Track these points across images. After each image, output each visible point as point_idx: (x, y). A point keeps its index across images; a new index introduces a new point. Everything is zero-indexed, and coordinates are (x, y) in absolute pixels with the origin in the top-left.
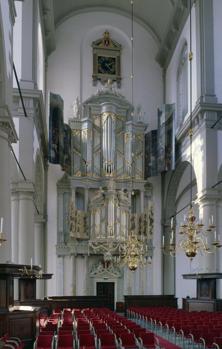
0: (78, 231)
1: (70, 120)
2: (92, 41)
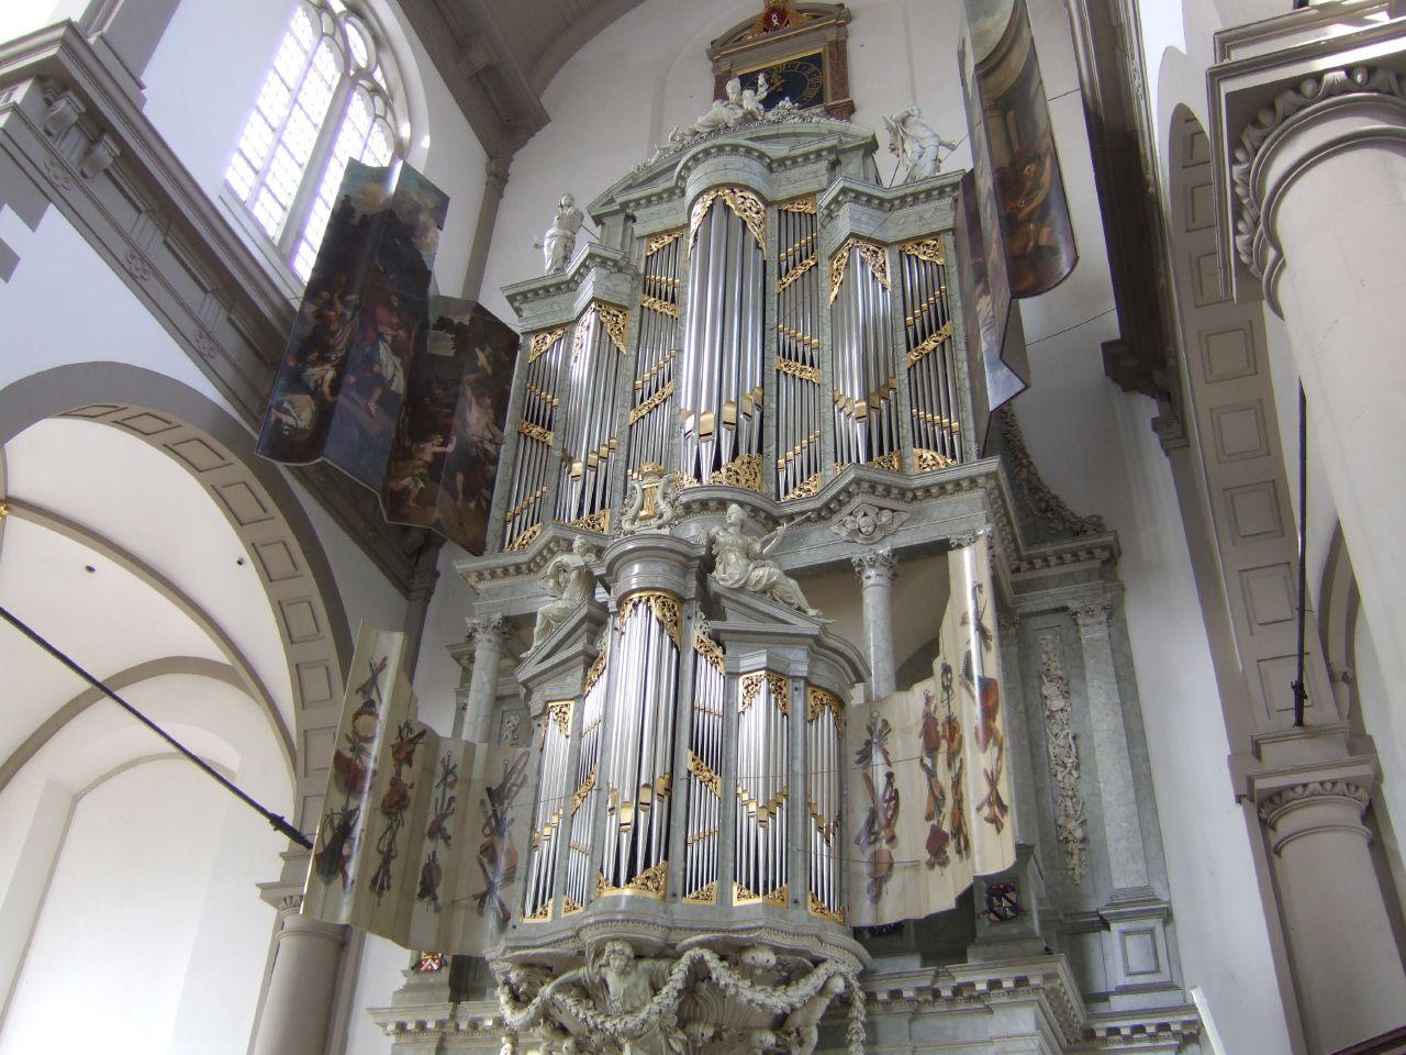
0: (428, 890)
1: (513, 292)
2: (710, 41)
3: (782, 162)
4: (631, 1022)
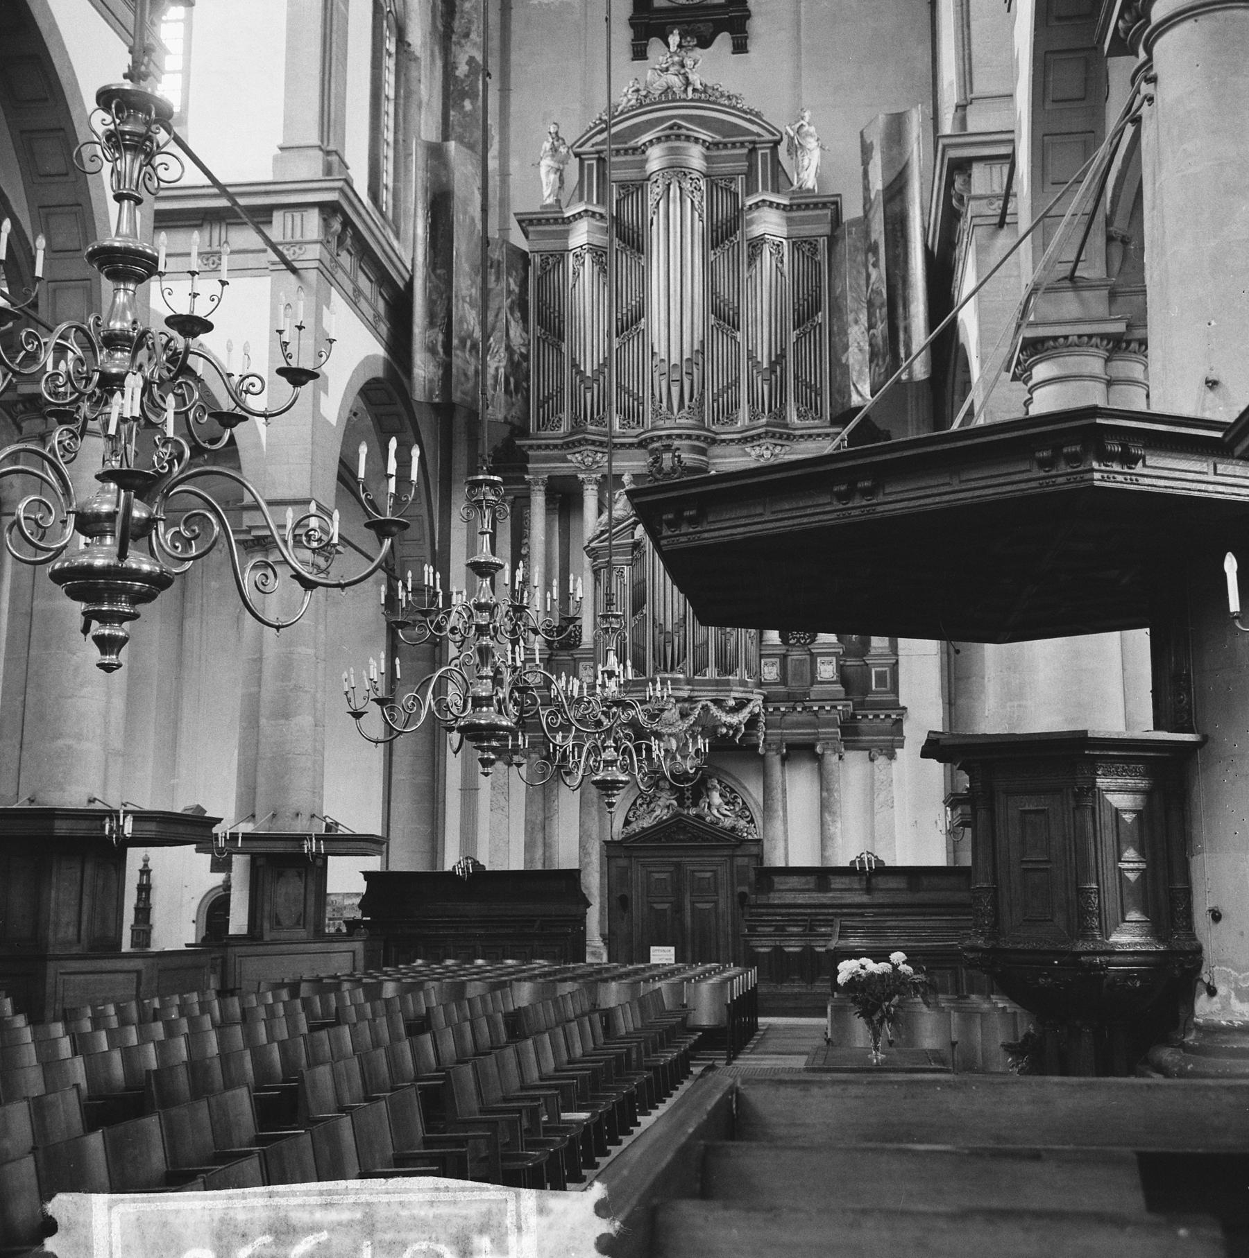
3: (716, 144)
4: (674, 730)
